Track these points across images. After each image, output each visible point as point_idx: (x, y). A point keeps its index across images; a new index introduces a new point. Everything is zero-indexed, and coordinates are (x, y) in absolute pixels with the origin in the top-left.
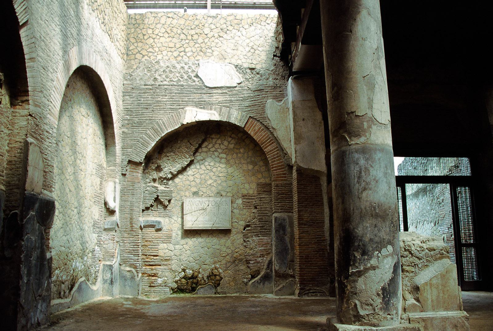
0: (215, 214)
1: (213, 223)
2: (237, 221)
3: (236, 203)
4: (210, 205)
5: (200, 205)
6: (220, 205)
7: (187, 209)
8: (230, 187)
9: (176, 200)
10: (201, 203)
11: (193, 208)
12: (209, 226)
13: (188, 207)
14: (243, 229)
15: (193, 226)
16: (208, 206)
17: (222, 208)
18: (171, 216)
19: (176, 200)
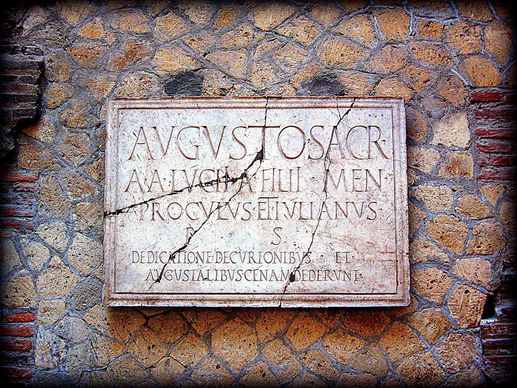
0: (306, 214)
1: (288, 268)
2: (445, 257)
3: (435, 141)
4: (271, 152)
5: (206, 149)
6: (334, 154)
7: (125, 180)
8: (392, 43)
9: (65, 123)
10: (215, 139)
11: (164, 172)
12: (263, 286)
13: (131, 165)
14: (480, 307)
15: (158, 287)
16: (260, 156)
17: (348, 175)
18: (31, 222)
19: (65, 123)
